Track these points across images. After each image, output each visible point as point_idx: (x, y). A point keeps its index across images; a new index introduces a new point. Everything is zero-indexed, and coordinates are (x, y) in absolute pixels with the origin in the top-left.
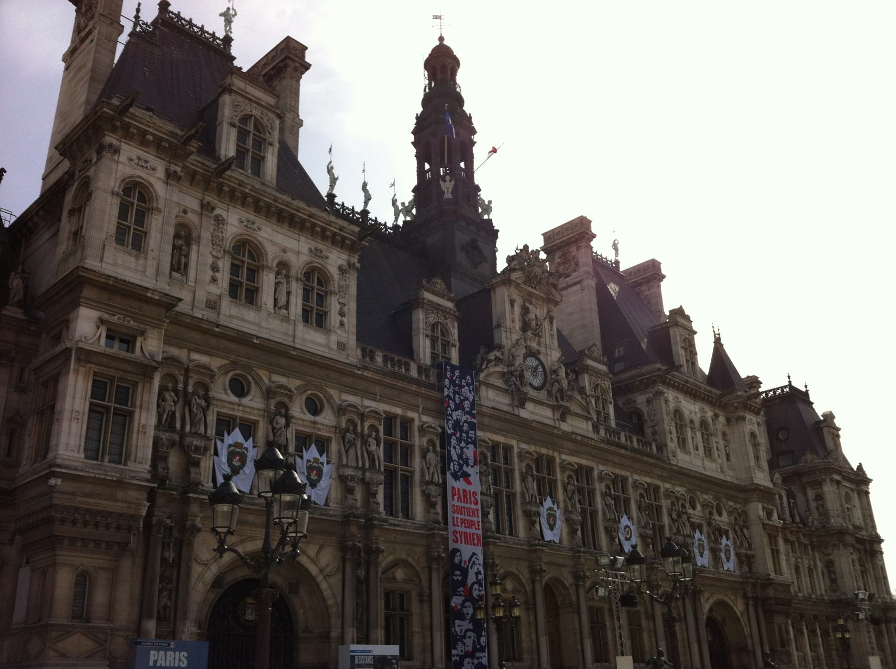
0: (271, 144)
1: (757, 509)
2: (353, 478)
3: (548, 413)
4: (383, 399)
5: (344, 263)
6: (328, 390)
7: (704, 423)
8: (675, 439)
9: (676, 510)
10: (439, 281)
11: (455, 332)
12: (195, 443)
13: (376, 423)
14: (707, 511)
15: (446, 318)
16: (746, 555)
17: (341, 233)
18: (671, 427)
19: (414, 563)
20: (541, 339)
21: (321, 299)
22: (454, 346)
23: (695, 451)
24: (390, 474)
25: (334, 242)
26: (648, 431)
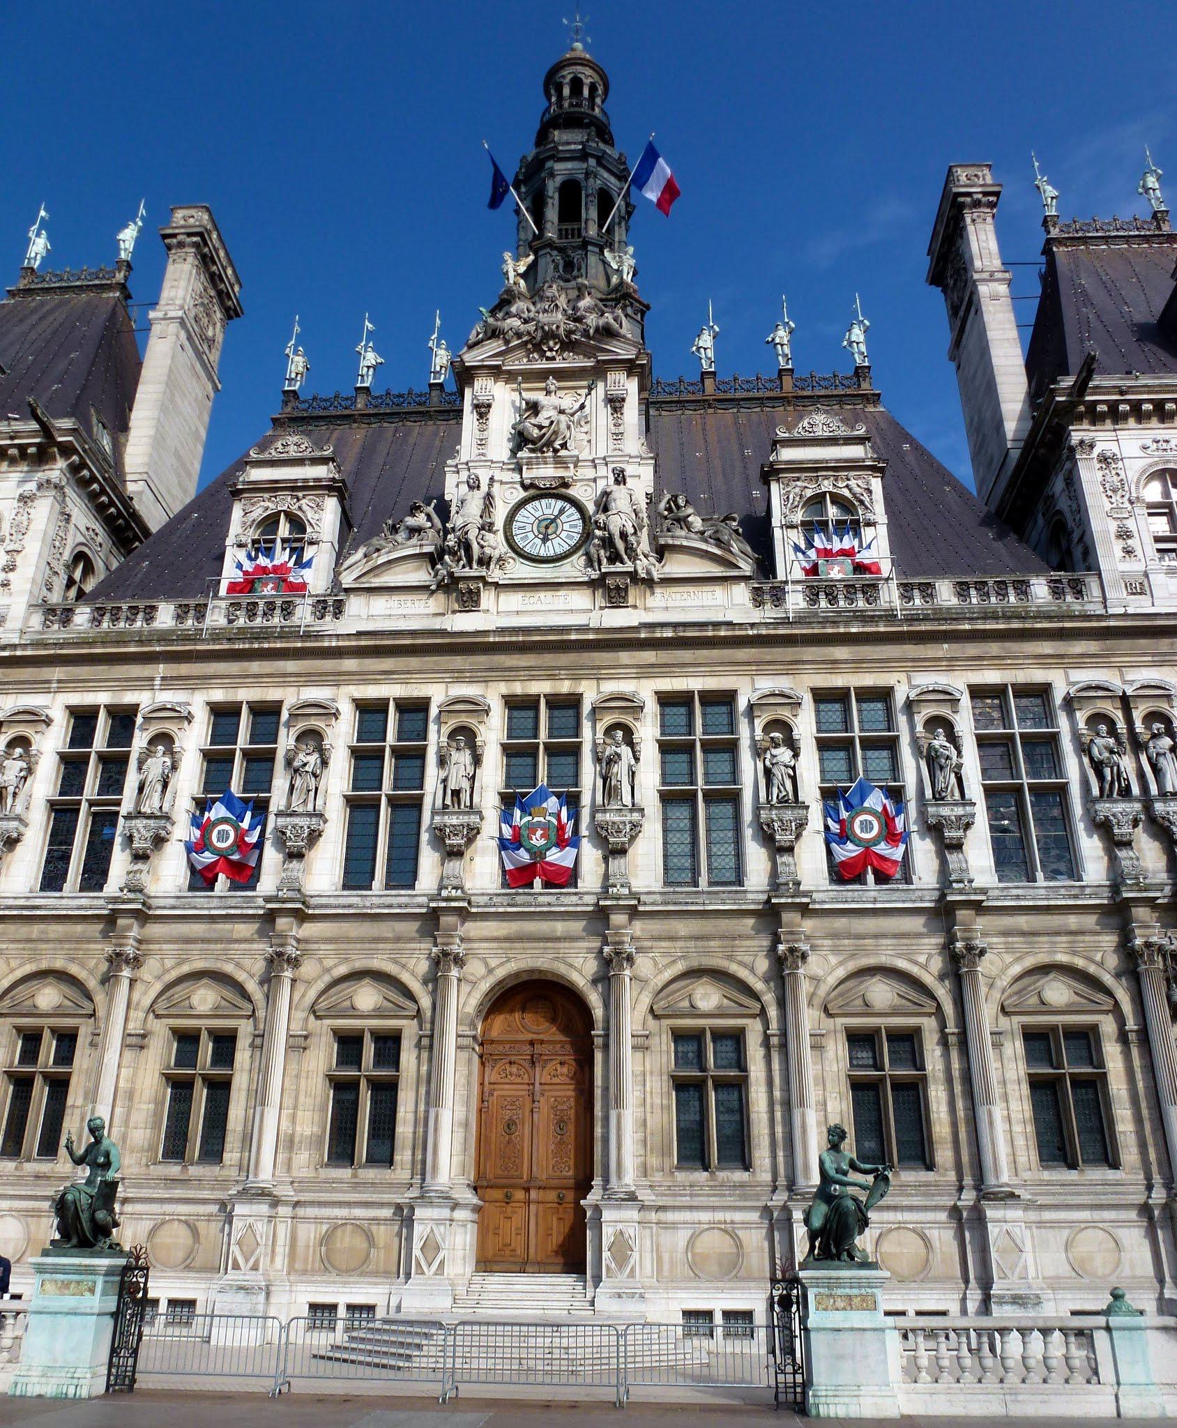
3: (580, 600)
5: (31, 486)
9: (1112, 732)
10: (296, 439)
15: (298, 500)
17: (16, 441)
18: (1130, 524)
20: (563, 453)
22: (311, 543)
24: (63, 815)
26: (1078, 552)
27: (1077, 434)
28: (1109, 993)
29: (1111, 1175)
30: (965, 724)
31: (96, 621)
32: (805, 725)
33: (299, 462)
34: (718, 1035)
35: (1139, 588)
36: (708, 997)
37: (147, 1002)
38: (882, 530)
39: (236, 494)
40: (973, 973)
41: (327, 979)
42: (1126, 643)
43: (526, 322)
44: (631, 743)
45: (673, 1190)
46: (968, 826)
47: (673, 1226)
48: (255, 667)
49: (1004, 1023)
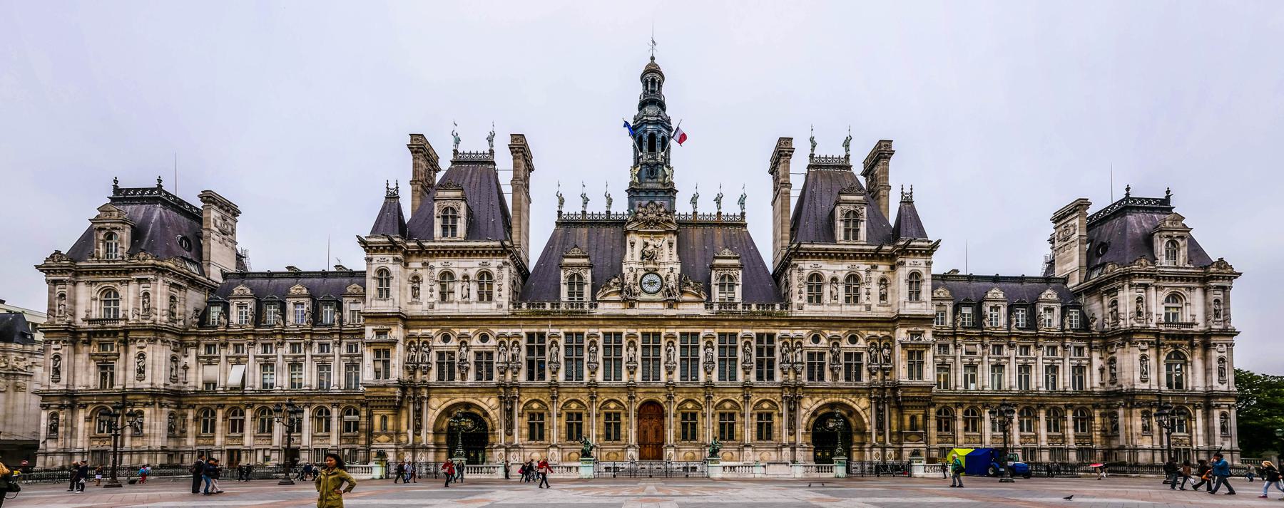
0: (459, 217)
1: (902, 334)
2: (502, 367)
3: (660, 306)
4: (524, 326)
5: (501, 263)
6: (491, 329)
7: (853, 278)
8: (805, 295)
9: (788, 346)
11: (588, 276)
12: (423, 365)
13: (518, 340)
14: (831, 343)
16: (883, 370)
19: (543, 400)
20: (656, 261)
21: (490, 285)
23: (833, 301)
25: (494, 255)
27: (793, 262)
28: (777, 406)
29: (771, 442)
30: (754, 343)
31: (528, 307)
32: (716, 343)
33: (579, 257)
34: (692, 414)
35: (800, 308)
36: (690, 406)
37: (560, 406)
38: (740, 286)
39: (561, 267)
40: (748, 402)
41: (603, 401)
42: (796, 322)
43: (644, 215)
44: (673, 346)
45: (681, 445)
46: (751, 368)
47: (681, 451)
48: (576, 322)
49: (754, 412)
